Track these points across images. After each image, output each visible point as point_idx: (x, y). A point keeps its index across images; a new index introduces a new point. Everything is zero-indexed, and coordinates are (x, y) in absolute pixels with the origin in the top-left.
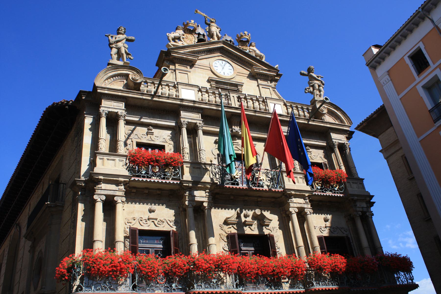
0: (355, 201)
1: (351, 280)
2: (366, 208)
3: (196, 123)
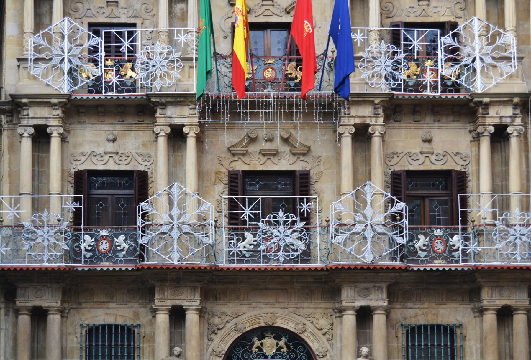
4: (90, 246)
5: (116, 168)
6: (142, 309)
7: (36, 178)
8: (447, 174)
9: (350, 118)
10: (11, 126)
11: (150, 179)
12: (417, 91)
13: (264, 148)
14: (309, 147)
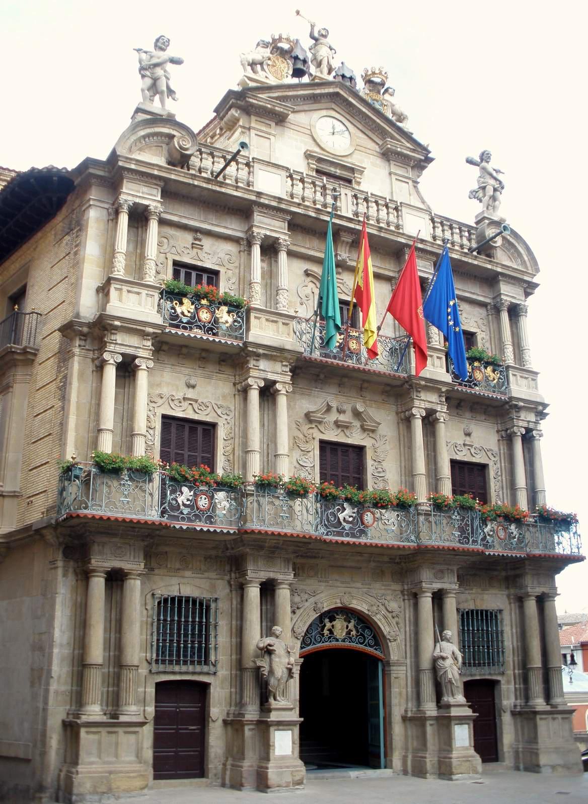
0: (518, 409)
1: (488, 537)
3: (278, 239)
4: (188, 500)
6: (220, 581)
10: (83, 351)
12: (470, 387)
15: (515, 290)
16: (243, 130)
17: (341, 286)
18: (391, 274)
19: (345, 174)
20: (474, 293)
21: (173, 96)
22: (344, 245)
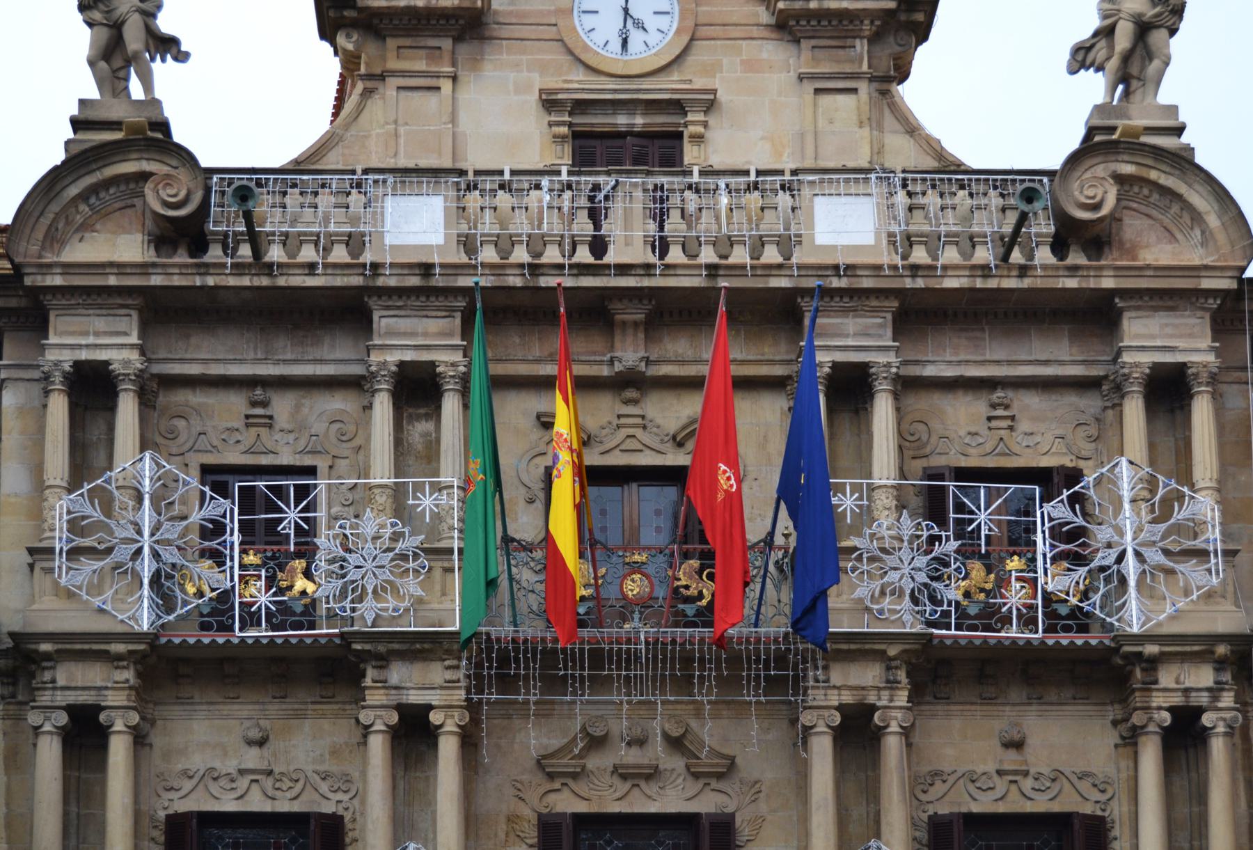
2: (1209, 690)
3: (433, 364)
5: (267, 807)
7: (73, 830)
8: (1060, 822)
9: (829, 692)
10: (11, 707)
11: (350, 834)
13: (625, 761)
14: (732, 759)
15: (1175, 326)
16: (370, 84)
17: (638, 432)
18: (779, 371)
19: (661, 121)
20: (1047, 362)
21: (174, 50)
22: (630, 331)
